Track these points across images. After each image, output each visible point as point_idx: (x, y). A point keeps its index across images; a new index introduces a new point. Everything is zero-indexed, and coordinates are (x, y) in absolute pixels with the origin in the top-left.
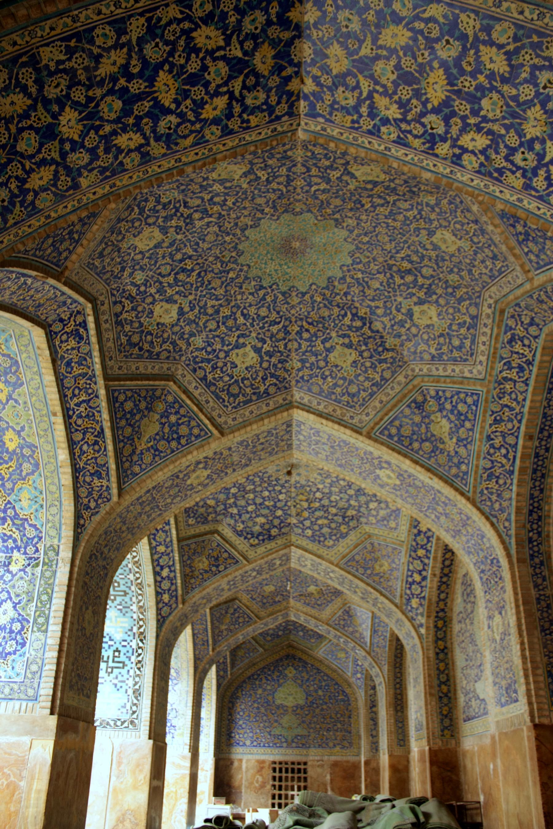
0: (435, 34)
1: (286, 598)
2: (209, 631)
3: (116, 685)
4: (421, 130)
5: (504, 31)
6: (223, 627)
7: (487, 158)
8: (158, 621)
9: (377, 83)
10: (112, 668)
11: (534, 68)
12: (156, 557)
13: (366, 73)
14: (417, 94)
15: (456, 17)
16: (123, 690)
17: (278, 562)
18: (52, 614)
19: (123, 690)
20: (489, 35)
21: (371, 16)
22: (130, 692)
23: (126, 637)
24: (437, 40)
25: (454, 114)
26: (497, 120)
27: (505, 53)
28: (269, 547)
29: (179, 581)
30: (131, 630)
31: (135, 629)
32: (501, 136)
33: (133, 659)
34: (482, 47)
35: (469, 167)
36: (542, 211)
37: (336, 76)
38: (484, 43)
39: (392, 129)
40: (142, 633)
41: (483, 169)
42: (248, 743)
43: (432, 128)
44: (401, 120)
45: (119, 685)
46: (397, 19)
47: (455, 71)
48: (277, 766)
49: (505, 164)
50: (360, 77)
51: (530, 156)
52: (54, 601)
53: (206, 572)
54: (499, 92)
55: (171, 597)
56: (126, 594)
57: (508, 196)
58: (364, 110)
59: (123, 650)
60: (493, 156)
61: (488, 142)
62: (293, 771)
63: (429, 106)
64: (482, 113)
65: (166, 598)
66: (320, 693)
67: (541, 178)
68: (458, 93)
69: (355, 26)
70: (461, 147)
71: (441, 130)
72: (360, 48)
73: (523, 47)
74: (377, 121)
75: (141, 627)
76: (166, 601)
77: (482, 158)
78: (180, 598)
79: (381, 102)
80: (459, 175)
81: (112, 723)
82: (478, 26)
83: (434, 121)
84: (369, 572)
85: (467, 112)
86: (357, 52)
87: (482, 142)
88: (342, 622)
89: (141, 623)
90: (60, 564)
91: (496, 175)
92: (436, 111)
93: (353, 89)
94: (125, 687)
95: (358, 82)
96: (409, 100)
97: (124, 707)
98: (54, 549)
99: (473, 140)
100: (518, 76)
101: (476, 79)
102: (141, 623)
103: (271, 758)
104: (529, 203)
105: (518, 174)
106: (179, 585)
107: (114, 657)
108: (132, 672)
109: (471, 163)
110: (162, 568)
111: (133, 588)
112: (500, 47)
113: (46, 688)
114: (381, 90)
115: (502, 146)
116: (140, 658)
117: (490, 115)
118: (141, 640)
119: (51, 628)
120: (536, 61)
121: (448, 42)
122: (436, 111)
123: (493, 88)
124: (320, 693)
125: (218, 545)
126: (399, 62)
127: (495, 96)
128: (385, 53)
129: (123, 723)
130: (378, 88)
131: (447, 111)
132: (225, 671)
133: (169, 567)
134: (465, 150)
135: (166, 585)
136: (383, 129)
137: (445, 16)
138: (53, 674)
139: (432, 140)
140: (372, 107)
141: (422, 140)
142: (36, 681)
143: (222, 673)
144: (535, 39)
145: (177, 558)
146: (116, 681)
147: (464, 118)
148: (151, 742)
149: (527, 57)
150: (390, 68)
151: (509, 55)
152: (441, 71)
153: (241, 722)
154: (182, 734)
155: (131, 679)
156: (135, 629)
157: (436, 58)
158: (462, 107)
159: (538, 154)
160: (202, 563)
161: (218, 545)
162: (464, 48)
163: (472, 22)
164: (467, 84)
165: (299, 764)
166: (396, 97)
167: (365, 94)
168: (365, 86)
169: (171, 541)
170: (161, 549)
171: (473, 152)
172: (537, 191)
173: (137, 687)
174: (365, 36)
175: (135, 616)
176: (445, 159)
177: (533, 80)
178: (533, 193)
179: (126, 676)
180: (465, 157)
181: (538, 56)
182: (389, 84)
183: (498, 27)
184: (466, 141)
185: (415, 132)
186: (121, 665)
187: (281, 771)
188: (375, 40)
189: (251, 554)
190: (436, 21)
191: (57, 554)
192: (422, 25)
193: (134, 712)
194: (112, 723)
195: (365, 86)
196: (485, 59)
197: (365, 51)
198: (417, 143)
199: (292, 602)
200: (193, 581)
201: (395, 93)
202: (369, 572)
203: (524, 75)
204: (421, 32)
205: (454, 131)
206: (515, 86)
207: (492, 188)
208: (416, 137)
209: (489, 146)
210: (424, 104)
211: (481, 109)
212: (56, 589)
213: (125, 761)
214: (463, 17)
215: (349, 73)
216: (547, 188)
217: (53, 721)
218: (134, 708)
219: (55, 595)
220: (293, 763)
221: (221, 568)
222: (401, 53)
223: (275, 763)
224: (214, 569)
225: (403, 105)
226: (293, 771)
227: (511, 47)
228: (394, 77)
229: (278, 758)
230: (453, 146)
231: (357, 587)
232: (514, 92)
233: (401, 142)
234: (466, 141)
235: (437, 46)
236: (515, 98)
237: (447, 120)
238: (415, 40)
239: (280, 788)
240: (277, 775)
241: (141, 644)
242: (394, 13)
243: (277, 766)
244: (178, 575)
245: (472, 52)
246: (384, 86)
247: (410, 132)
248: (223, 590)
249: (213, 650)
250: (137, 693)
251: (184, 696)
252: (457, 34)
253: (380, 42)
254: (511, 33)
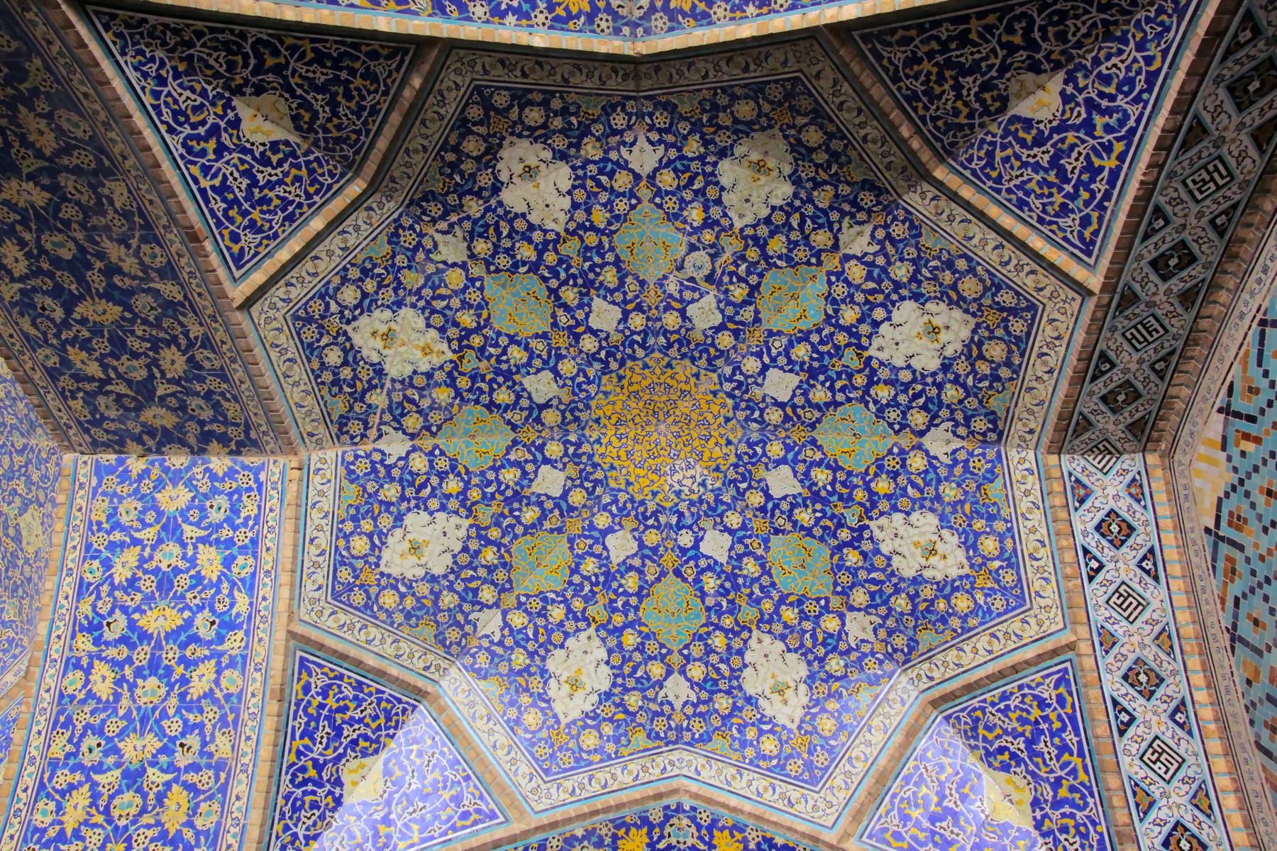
0: (220, 608)
4: (104, 611)
5: (233, 682)
7: (83, 702)
9: (154, 548)
11: (201, 726)
13: (163, 534)
14: (149, 599)
15: (239, 627)
20: (228, 667)
21: (226, 533)
24: (213, 611)
25: (132, 647)
26: (134, 701)
27: (211, 690)
32: (115, 711)
34: (213, 662)
35: (65, 683)
36: (23, 795)
37: (154, 499)
38: (219, 663)
39: (99, 574)
41: (67, 700)
43: (109, 624)
44: (112, 584)
46: (228, 562)
47: (183, 638)
49: (79, 726)
50: (158, 527)
51: (97, 755)
54: (168, 694)
57: (35, 744)
58: (117, 536)
60: (87, 709)
61: (104, 698)
63: (136, 616)
64: (140, 681)
67: (69, 779)
68: (158, 646)
69: (215, 516)
70: (91, 666)
71: (108, 635)
72: (191, 524)
73: (221, 707)
74: (106, 554)
77: (82, 696)
79: (131, 556)
80: (52, 671)
82: (233, 653)
83: (120, 624)
85: (137, 663)
86: (186, 520)
87: (103, 689)
91: (62, 719)
92: (132, 625)
93: (142, 521)
95: (150, 525)
96: (139, 590)
99: (104, 678)
100: (189, 710)
101: (178, 664)
104: (30, 775)
105: (69, 748)
109: (72, 683)
112: (217, 682)
114: (146, 554)
115: (103, 716)
117: (138, 692)
120: (209, 726)
121: (213, 623)
122: (132, 625)
123: (171, 686)
126: (182, 571)
127: (163, 690)
128: (190, 553)
130: (148, 550)
131: (135, 638)
134: (88, 671)
136: (96, 563)
137: (238, 615)
139: (93, 627)
140: (123, 545)
141: (91, 615)
144: (230, 718)
147: (129, 660)
149: (211, 715)
150: (174, 562)
151: (209, 695)
152: (180, 622)
157: (194, 614)
158: (142, 655)
159: (101, 763)
162: (210, 643)
163: (237, 644)
164: (171, 655)
166: (140, 574)
167: (137, 535)
168: (149, 534)
171: (87, 682)
172: (50, 780)
174: (205, 529)
176: (71, 649)
177: (188, 729)
178: (47, 775)
180: (79, 674)
181: (214, 726)
182: (154, 564)
183: (236, 673)
184: (101, 669)
185: (100, 604)
188: (203, 540)
190: (232, 605)
192: (226, 592)
195: (149, 534)
196: (202, 668)
197: (189, 531)
198: (86, 608)
201: (146, 572)
203: (191, 717)
204: (219, 592)
205: (111, 652)
206: (178, 711)
207: (42, 719)
208: (94, 606)
209: (99, 700)
210: (138, 609)
211: (144, 678)
214: (241, 634)
215: (160, 514)
216: (57, 791)
222: (192, 572)
225: (132, 583)
227: (219, 695)
228: (164, 567)
230: (91, 657)
232: (171, 712)
233: (83, 588)
234: (101, 669)
235: (206, 612)
236: (164, 714)
237: (123, 640)
238: (211, 585)
242: (234, 558)
245: (207, 653)
246: (151, 558)
247: (99, 597)
252: (223, 632)
253: (200, 546)
254: (233, 690)
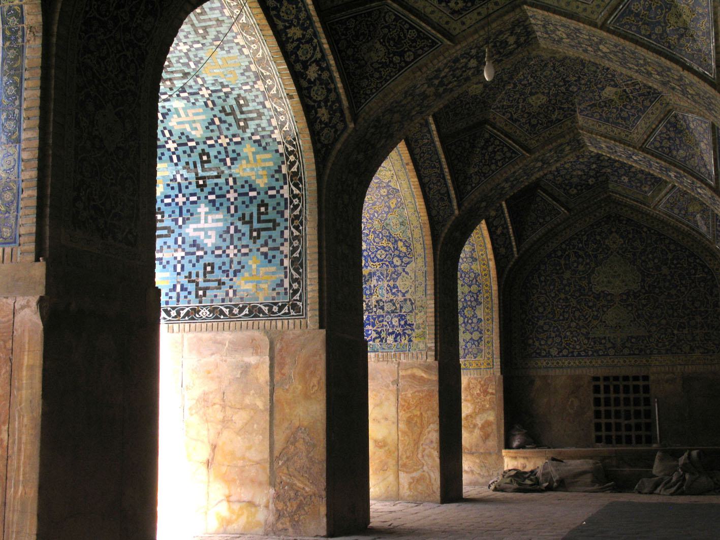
1: (570, 114)
2: (448, 177)
3: (265, 255)
6: (472, 171)
8: (317, 152)
10: (259, 231)
12: (290, 47)
16: (277, 261)
17: (512, 40)
18: (24, 115)
19: (277, 261)
22: (287, 262)
23: (274, 184)
28: (484, 11)
29: (340, 85)
30: (279, 171)
31: (284, 169)
33: (287, 214)
40: (295, 174)
42: (554, 352)
45: (271, 254)
48: (602, 384)
52: (25, 94)
53: (384, 65)
55: (332, 113)
56: (260, 115)
59: (272, 203)
62: (626, 388)
65: (323, 113)
66: (665, 270)
75: (292, 164)
76: (325, 118)
78: (347, 113)
81: (266, 309)
84: (658, 30)
88: (666, 144)
89: (292, 158)
90: (28, 35)
94: (279, 257)
97: (281, 284)
98: (16, 14)
102: (292, 158)
103: (592, 372)
106: (341, 91)
107: (260, 213)
108: (287, 234)
110: (305, 66)
111: (268, 104)
113: (27, 224)
116: (297, 212)
118: (296, 185)
119: (24, 136)
124: (665, 270)
125: (397, 18)
129: (281, 308)
132: (509, 247)
133: (317, 62)
135: (318, 93)
138: (34, 202)
142: (13, 214)
143: (503, 251)
145: (326, 46)
146: (264, 249)
148: (323, 332)
153: (541, 323)
154: (423, 335)
155: (287, 244)
156: (284, 169)
160: (377, 53)
161: (397, 18)
165: (636, 378)
169: (309, 17)
170: (295, 32)
173: (296, 255)
175: (281, 149)
179: (279, 240)
186: (270, 225)
187: (607, 389)
189: (456, 27)
191: (21, 20)
193: (295, 292)
194: (266, 309)
199: (581, 120)
200: (365, 83)
202: (658, 30)
212: (26, 75)
213: (288, 360)
217: (39, 270)
218: (295, 286)
219: (25, 85)
220: (626, 378)
221: (409, 56)
223: (596, 379)
224: (396, 59)
226: (626, 389)
229: (601, 372)
231: (646, 63)
239: (608, 415)
240: (602, 396)
241: (296, 191)
243: (602, 384)
244: (336, 75)
248: (424, 96)
249: (459, 206)
250: (298, 264)
251: (421, 279)
